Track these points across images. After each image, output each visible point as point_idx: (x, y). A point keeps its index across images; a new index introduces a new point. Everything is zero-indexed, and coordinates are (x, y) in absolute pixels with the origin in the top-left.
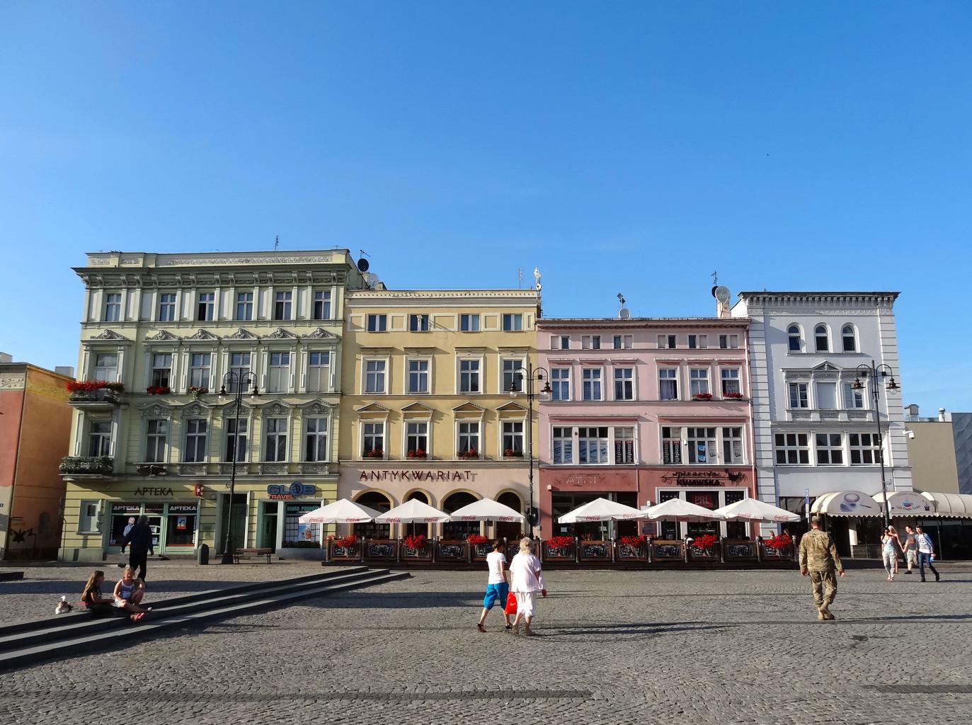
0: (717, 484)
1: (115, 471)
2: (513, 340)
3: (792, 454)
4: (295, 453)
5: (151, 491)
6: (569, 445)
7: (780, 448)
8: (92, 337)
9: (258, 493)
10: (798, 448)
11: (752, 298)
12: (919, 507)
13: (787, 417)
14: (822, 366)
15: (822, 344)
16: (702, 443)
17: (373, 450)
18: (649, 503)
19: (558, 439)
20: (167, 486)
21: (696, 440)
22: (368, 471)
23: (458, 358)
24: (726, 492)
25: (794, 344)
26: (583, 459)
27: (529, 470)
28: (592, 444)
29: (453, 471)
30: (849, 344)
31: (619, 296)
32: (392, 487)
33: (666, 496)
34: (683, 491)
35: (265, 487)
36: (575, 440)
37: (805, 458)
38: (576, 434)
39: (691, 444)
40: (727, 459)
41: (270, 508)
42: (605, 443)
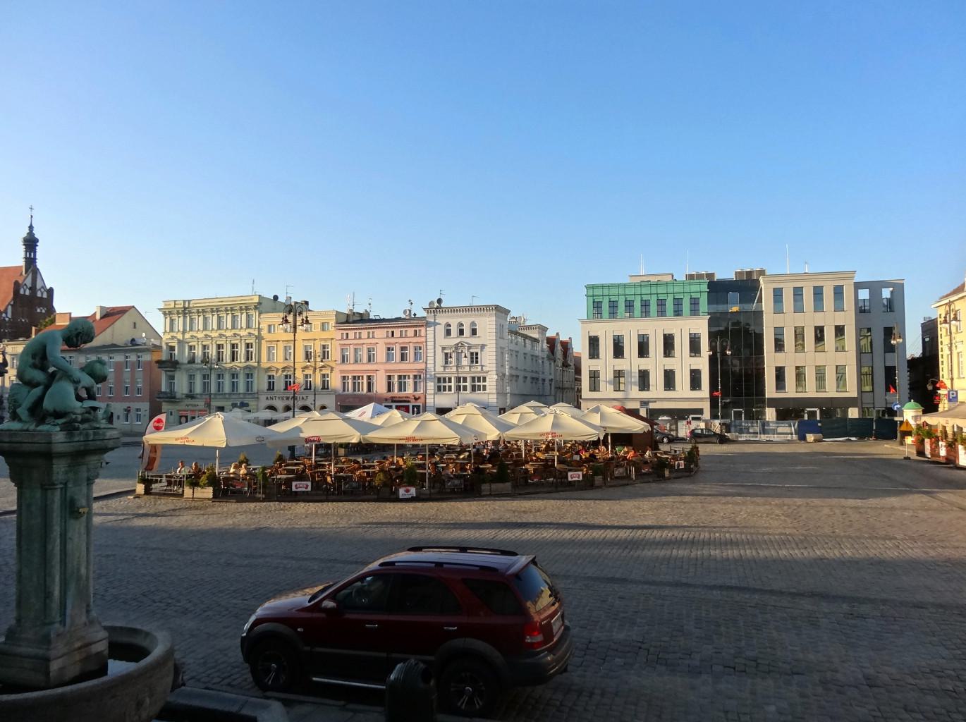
0: (409, 402)
1: (177, 397)
2: (325, 335)
7: (439, 384)
10: (447, 384)
13: (442, 369)
14: (458, 344)
15: (461, 332)
20: (196, 403)
22: (269, 396)
25: (448, 333)
30: (474, 332)
31: (410, 301)
34: (394, 405)
35: (230, 403)
36: (350, 381)
37: (450, 390)
40: (415, 390)
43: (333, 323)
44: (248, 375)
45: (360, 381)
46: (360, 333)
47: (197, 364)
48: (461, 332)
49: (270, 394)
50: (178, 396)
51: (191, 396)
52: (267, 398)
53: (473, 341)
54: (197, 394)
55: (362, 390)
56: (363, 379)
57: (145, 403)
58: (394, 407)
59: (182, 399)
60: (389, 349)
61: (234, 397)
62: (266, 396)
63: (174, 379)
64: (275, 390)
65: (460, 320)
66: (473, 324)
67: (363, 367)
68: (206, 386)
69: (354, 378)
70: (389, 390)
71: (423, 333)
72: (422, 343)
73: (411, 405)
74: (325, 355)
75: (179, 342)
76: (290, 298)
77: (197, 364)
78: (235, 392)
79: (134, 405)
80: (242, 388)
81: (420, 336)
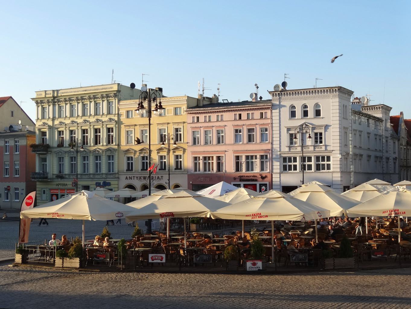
0: (256, 180)
1: (49, 177)
2: (178, 119)
3: (290, 166)
4: (104, 169)
8: (39, 125)
10: (292, 164)
11: (273, 94)
13: (287, 149)
14: (302, 125)
15: (306, 114)
20: (65, 183)
23: (158, 128)
24: (260, 184)
30: (318, 113)
34: (242, 183)
35: (94, 183)
36: (201, 162)
37: (295, 168)
38: (201, 159)
40: (262, 169)
43: (184, 107)
44: (109, 157)
45: (211, 161)
46: (209, 117)
47: (66, 147)
48: (306, 114)
49: (129, 174)
50: (50, 176)
51: (60, 176)
52: (127, 178)
53: (317, 122)
54: (65, 175)
55: (212, 170)
56: (213, 160)
57: (22, 183)
58: (242, 185)
59: (53, 179)
60: (236, 131)
61: (97, 177)
62: (125, 176)
63: (46, 161)
64: (134, 171)
65: (304, 102)
66: (317, 105)
67: (213, 149)
68: (73, 167)
69: (205, 158)
70: (237, 169)
71: (269, 115)
72: (268, 124)
73: (258, 184)
74: (178, 138)
75: (50, 128)
76: (146, 85)
77: (66, 147)
78: (98, 173)
79: (13, 185)
80: (104, 169)
81: (266, 118)
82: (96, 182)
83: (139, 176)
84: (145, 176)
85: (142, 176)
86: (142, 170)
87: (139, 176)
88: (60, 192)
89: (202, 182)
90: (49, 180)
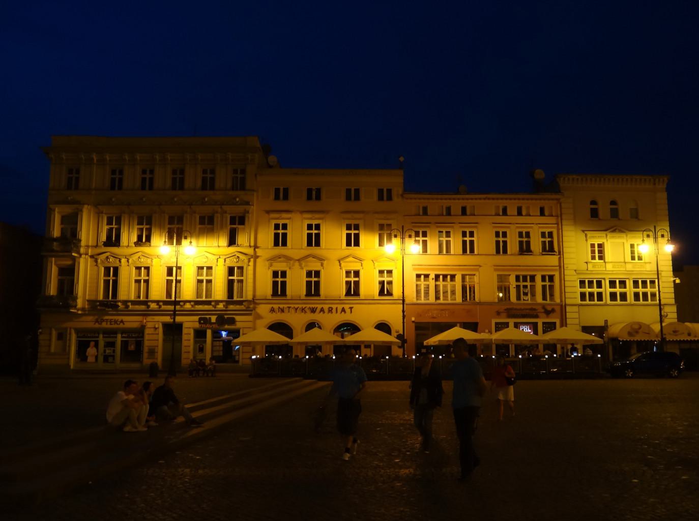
0: (537, 317)
3: (591, 294)
5: (107, 322)
6: (427, 287)
9: (190, 323)
10: (595, 290)
12: (683, 333)
16: (525, 287)
17: (279, 289)
18: (487, 331)
19: (418, 283)
21: (522, 284)
22: (276, 307)
26: (437, 298)
27: (402, 305)
28: (445, 286)
29: (340, 307)
32: (297, 321)
33: (500, 327)
34: (511, 322)
35: (197, 318)
36: (432, 283)
39: (518, 287)
40: (544, 298)
41: (200, 334)
42: (454, 286)
52: (272, 310)
73: (540, 322)
78: (204, 299)
82: (200, 316)
83: (300, 306)
84: (313, 306)
85: (308, 306)
86: (307, 295)
87: (300, 306)
88: (104, 337)
89: (434, 318)
90: (80, 312)
